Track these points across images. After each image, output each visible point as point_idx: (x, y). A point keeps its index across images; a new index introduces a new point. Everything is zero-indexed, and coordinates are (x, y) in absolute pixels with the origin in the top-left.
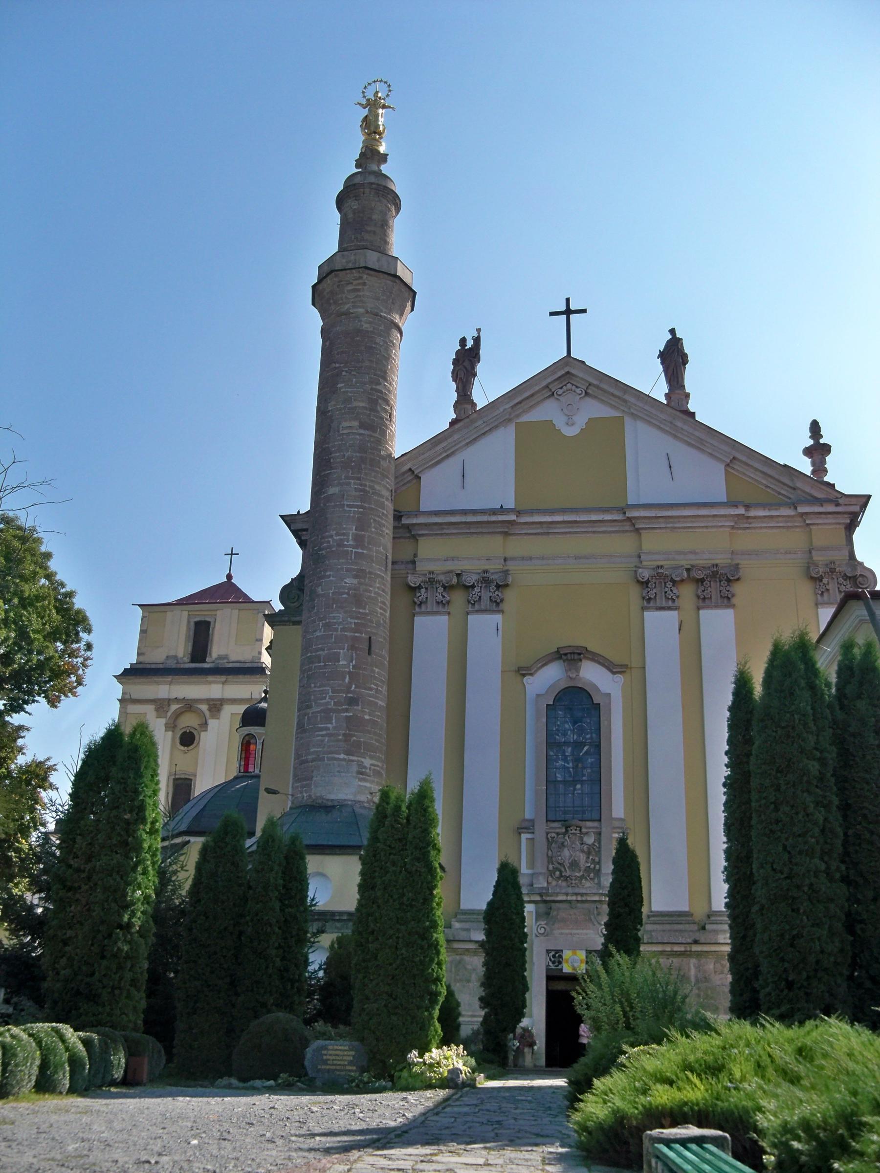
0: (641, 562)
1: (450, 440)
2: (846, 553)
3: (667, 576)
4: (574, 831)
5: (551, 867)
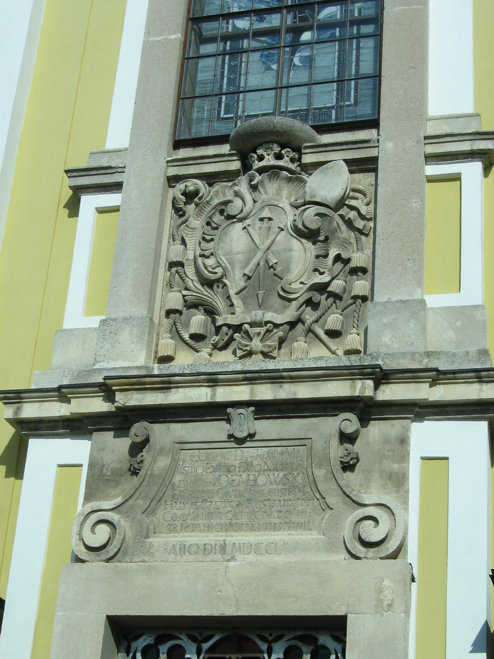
4: (269, 161)
5: (175, 300)
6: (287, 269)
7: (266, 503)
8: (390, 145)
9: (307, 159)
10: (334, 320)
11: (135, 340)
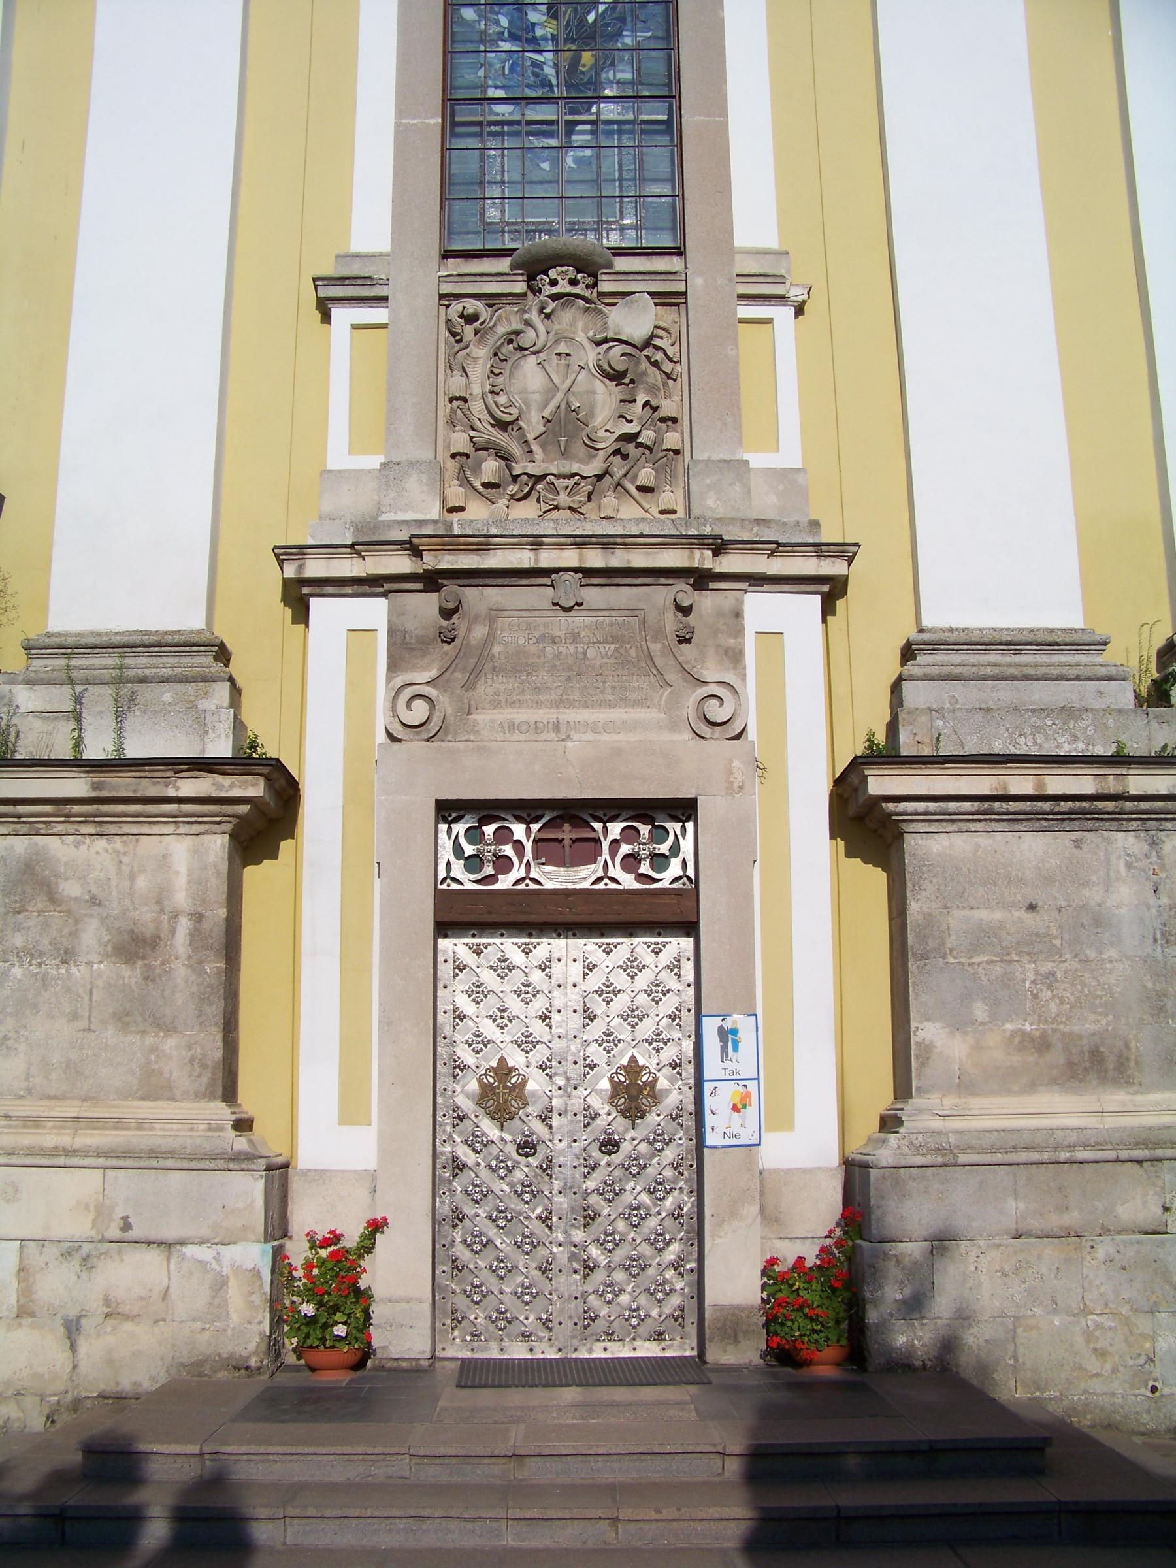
4: (563, 287)
5: (460, 441)
6: (591, 414)
7: (599, 678)
8: (699, 281)
9: (605, 286)
10: (646, 475)
11: (425, 488)
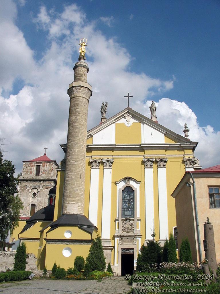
0: (144, 157)
1: (100, 127)
2: (192, 155)
3: (150, 160)
5: (123, 228)
10: (132, 231)
